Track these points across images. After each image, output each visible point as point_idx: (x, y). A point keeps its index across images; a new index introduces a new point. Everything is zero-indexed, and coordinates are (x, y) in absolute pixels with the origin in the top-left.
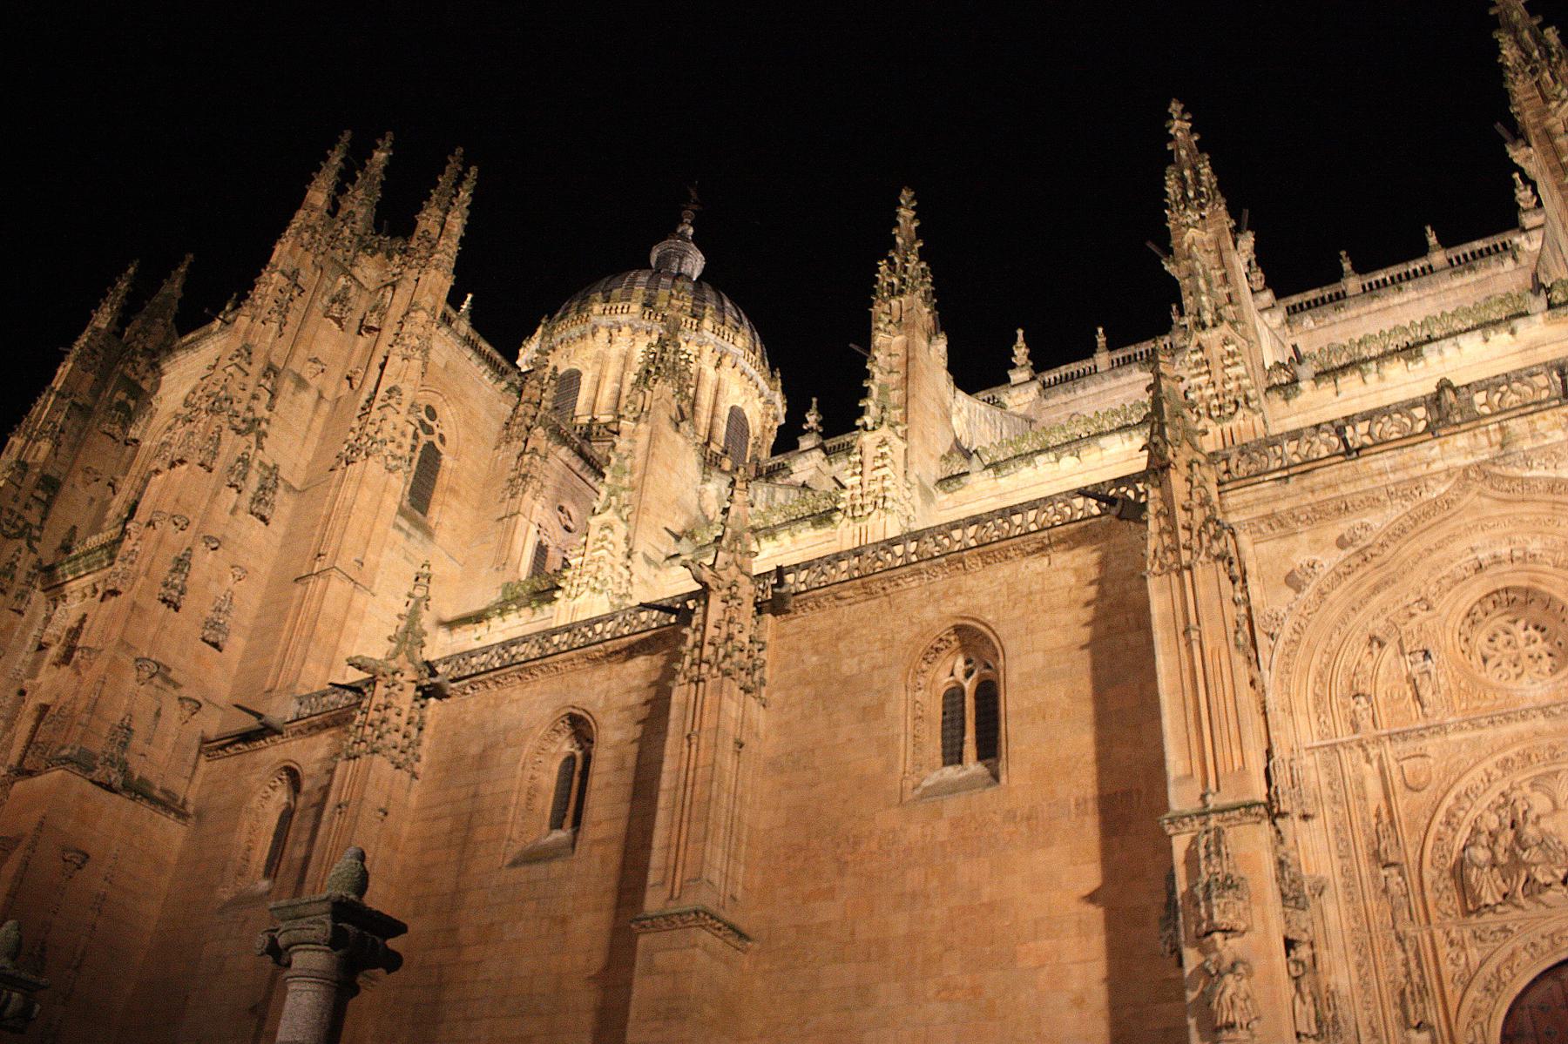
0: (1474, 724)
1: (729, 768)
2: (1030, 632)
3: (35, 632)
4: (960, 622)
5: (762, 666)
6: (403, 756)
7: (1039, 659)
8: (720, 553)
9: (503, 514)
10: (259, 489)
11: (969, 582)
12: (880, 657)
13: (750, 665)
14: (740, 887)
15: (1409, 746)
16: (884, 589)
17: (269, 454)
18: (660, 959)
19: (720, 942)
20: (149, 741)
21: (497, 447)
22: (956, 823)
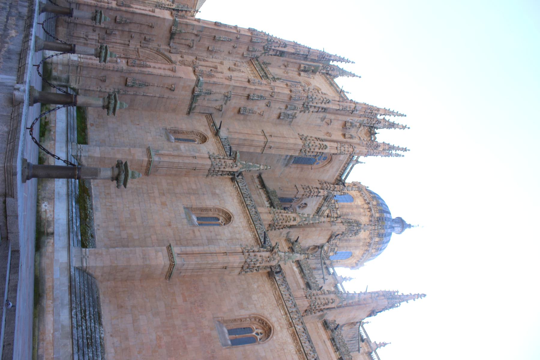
1: (218, 266)
2: (271, 351)
3: (238, 60)
4: (272, 329)
5: (251, 271)
6: (212, 171)
7: (263, 354)
8: (283, 253)
9: (297, 186)
10: (288, 114)
11: (285, 331)
13: (250, 268)
14: (184, 274)
16: (280, 304)
17: (299, 115)
18: (160, 254)
19: (167, 270)
20: (208, 100)
21: (319, 181)
22: (209, 335)
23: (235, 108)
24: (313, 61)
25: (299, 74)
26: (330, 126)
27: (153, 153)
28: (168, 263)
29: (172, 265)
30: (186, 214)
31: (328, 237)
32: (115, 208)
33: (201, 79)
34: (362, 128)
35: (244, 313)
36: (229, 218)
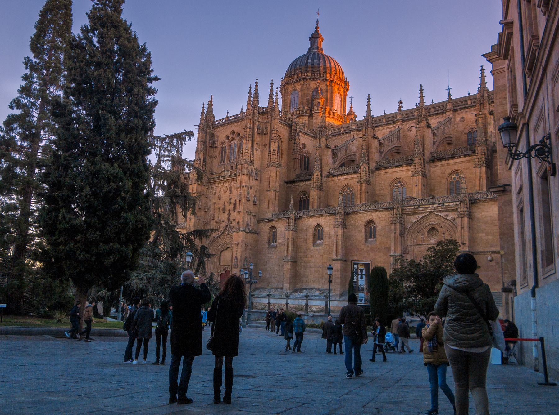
0: (426, 245)
12: (361, 223)
15: (420, 246)
18: (336, 264)
22: (370, 248)
23: (254, 207)
24: (206, 136)
25: (216, 147)
26: (260, 143)
27: (286, 260)
28: (340, 262)
29: (341, 260)
30: (316, 246)
31: (328, 149)
32: (313, 279)
33: (241, 229)
34: (260, 120)
35: (363, 231)
36: (319, 225)
